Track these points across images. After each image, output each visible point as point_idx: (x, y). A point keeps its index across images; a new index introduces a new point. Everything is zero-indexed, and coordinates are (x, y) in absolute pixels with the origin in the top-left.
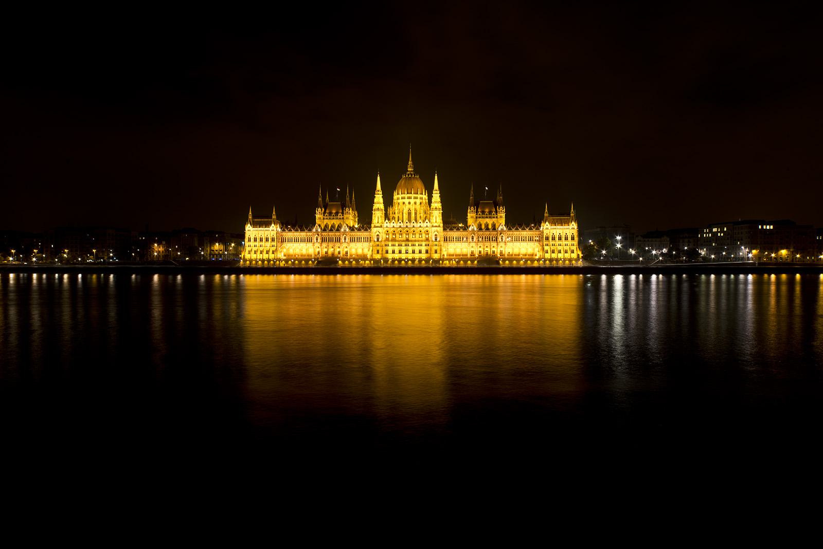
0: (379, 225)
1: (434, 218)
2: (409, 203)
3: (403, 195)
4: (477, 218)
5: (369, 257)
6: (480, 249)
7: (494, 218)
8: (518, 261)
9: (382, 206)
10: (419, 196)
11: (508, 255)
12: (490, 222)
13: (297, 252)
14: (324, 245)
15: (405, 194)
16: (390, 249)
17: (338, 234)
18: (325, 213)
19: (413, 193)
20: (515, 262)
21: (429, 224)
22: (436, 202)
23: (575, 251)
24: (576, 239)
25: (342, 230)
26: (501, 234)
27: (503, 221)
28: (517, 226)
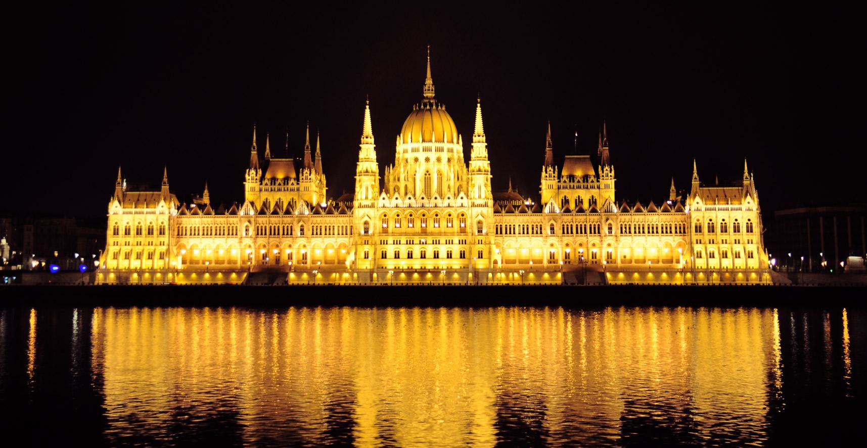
0: (369, 203)
1: (476, 189)
2: (427, 160)
3: (415, 145)
4: (559, 188)
5: (348, 264)
6: (568, 250)
7: (593, 187)
8: (643, 273)
9: (374, 166)
10: (446, 146)
11: (622, 262)
12: (585, 195)
13: (209, 254)
14: (261, 240)
15: (418, 142)
16: (390, 249)
17: (287, 219)
18: (262, 178)
19: (433, 140)
20: (636, 275)
21: (465, 201)
22: (479, 158)
23: (755, 254)
24: (757, 229)
25: (296, 213)
26: (607, 220)
27: (611, 194)
28: (638, 205)
